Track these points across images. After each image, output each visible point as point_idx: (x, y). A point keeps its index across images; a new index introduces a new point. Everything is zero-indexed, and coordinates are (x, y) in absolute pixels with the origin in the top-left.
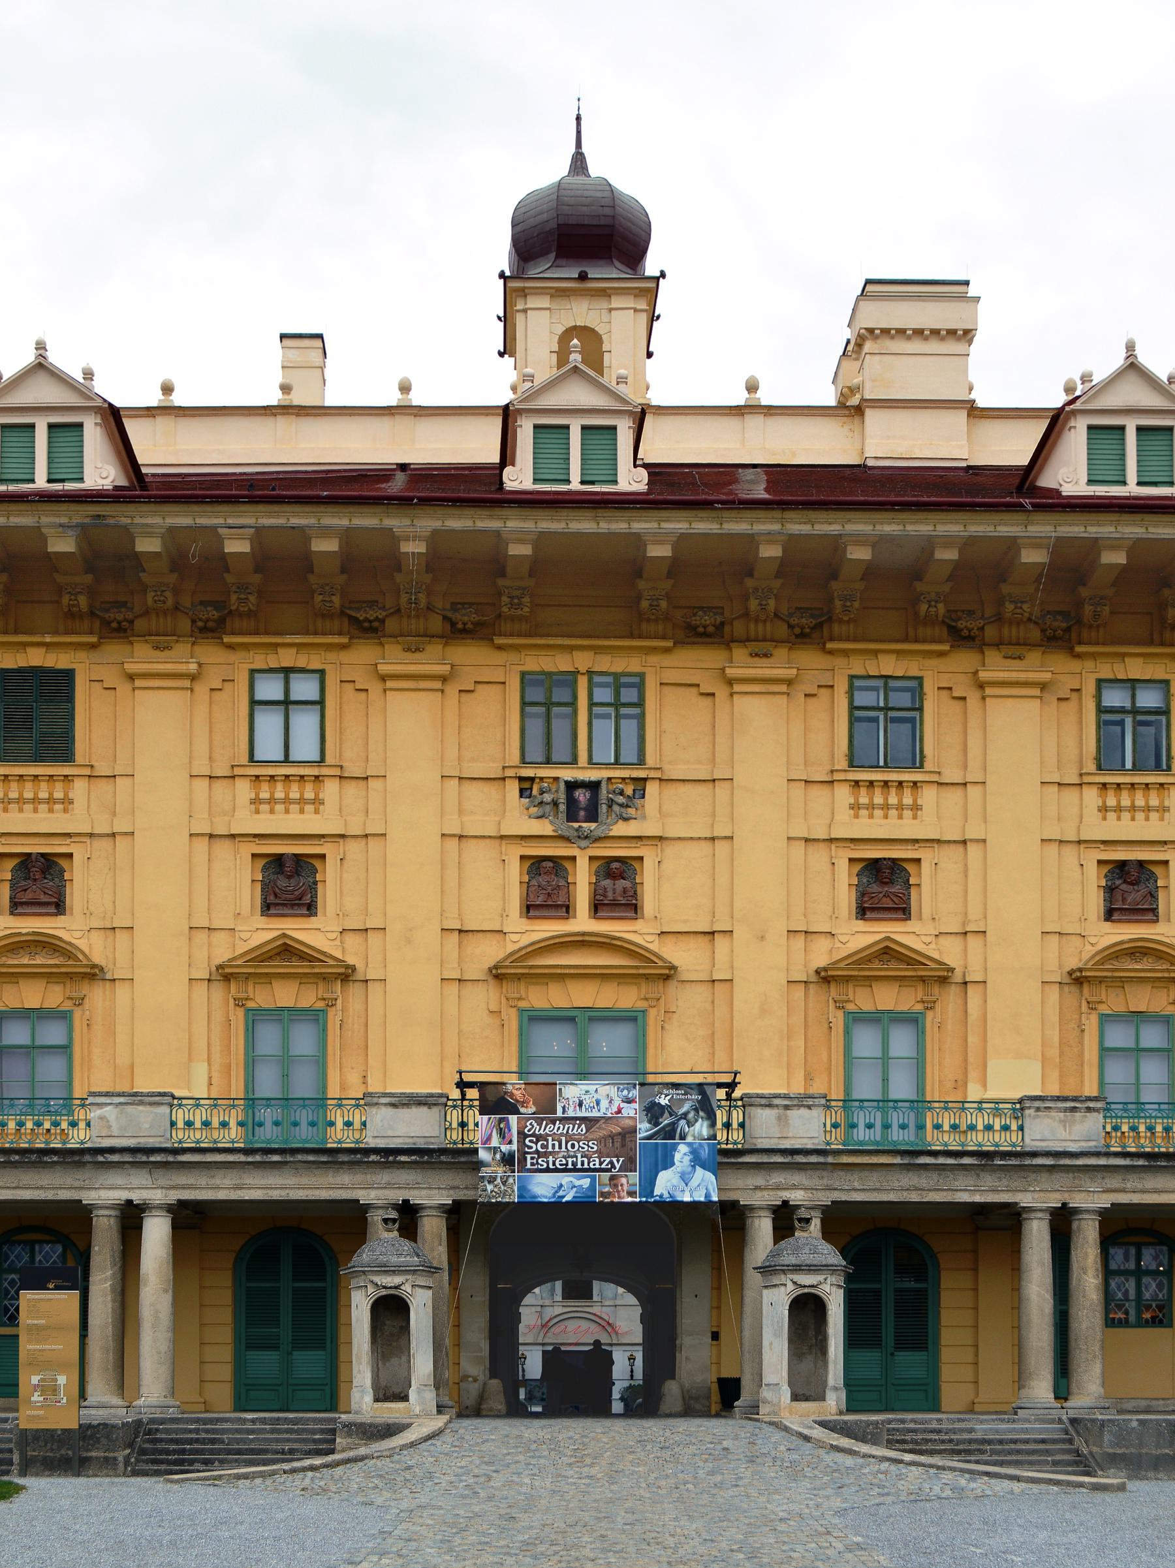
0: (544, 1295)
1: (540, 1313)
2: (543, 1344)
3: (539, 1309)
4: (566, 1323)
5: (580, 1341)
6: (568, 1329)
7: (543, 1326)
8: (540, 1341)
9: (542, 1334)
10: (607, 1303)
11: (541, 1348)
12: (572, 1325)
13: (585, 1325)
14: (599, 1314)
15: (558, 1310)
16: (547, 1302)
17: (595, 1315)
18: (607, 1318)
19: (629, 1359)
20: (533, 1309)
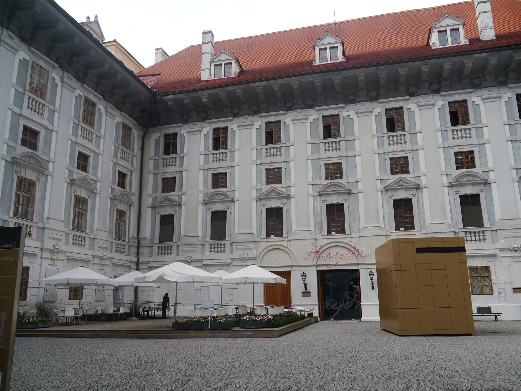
0: (316, 232)
1: (315, 245)
2: (317, 266)
3: (313, 241)
4: (329, 250)
5: (339, 263)
6: (332, 254)
7: (317, 253)
8: (315, 263)
9: (316, 259)
10: (354, 235)
11: (315, 268)
12: (333, 251)
13: (341, 251)
14: (349, 243)
15: (325, 242)
16: (319, 236)
17: (347, 244)
18: (354, 245)
19: (370, 275)
20: (310, 242)
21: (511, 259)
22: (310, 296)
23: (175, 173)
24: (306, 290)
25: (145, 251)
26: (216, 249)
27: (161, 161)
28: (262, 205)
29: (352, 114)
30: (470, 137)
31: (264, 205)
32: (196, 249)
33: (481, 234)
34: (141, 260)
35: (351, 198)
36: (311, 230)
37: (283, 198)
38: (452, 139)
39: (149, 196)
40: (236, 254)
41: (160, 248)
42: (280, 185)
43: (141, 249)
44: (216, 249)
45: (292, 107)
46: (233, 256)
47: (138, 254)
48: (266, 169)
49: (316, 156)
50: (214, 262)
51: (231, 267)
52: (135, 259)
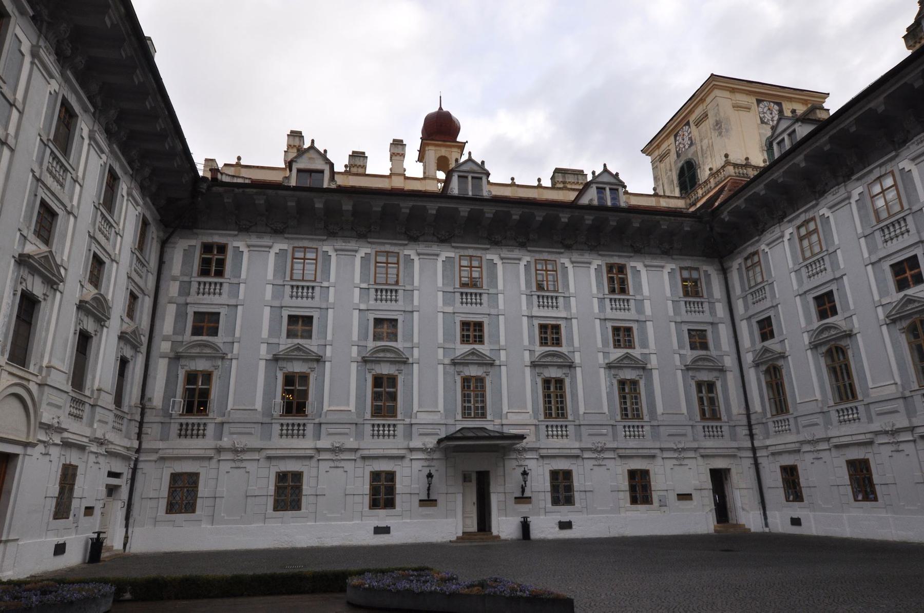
21: (675, 462)
22: (435, 505)
23: (219, 307)
24: (428, 497)
25: (152, 430)
26: (290, 432)
27: (195, 286)
28: (367, 371)
29: (496, 259)
30: (629, 310)
31: (370, 371)
32: (253, 431)
33: (564, 429)
34: (144, 446)
35: (492, 370)
36: (350, 411)
37: (312, 360)
38: (685, 311)
39: (166, 338)
40: (324, 443)
41: (184, 427)
42: (308, 341)
43: (145, 425)
44: (290, 432)
45: (418, 237)
46: (320, 444)
47: (139, 436)
48: (375, 319)
49: (450, 309)
50: (634, 452)
51: (313, 462)
52: (136, 444)
